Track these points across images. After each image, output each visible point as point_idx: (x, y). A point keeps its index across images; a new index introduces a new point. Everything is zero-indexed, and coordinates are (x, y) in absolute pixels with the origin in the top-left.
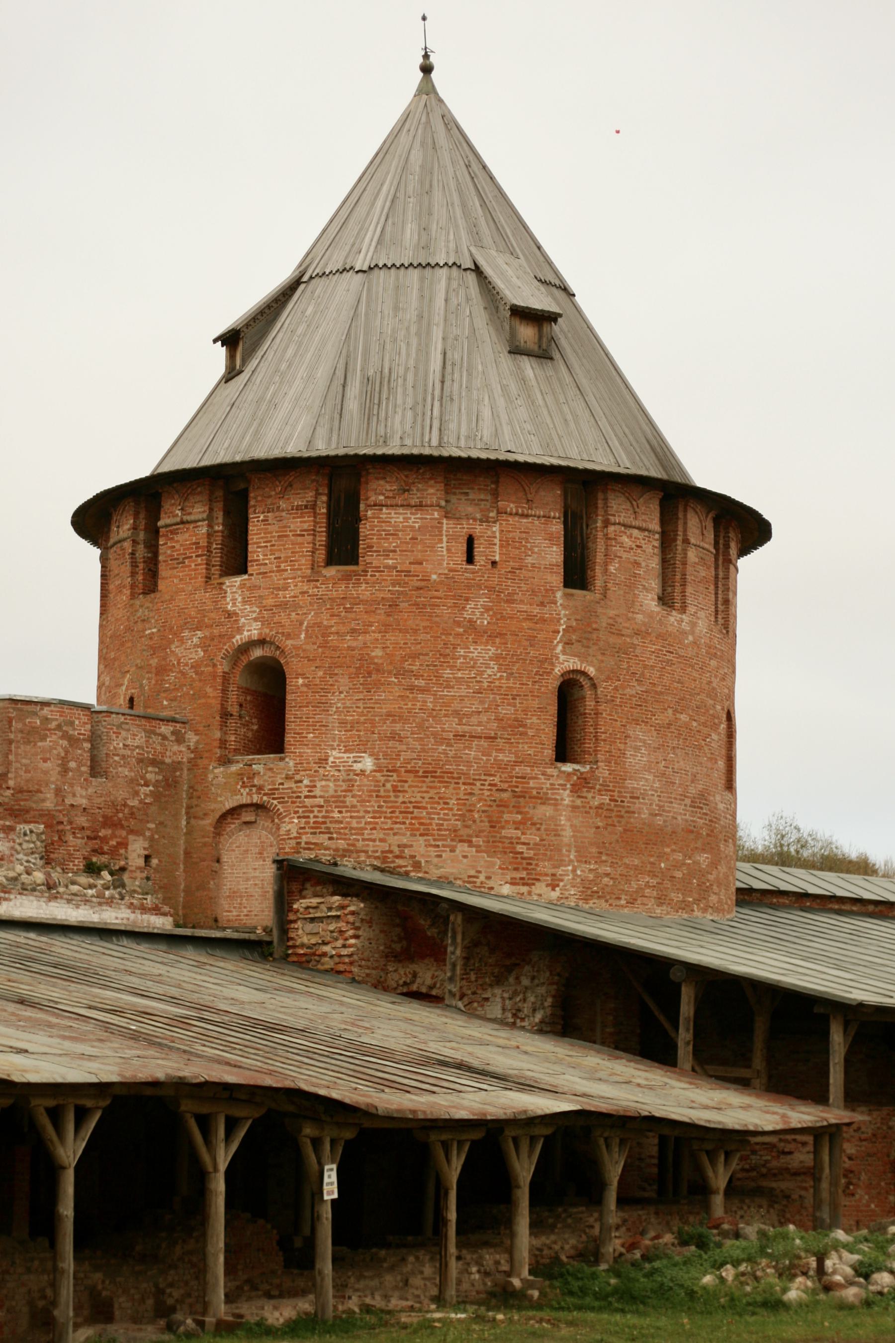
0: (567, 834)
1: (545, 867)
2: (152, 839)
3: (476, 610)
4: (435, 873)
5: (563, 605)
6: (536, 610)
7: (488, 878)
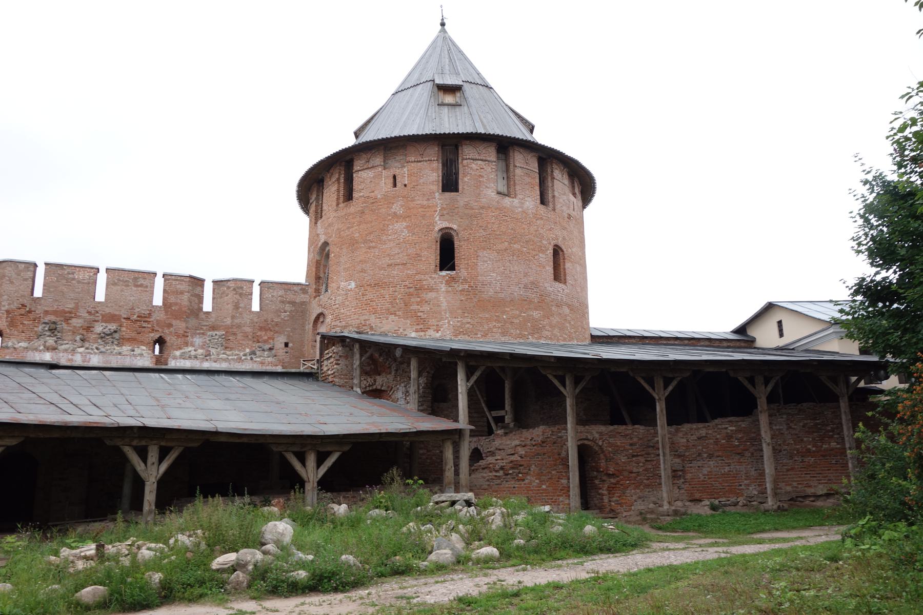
0: (444, 305)
1: (433, 322)
2: (289, 336)
3: (397, 208)
4: (379, 331)
5: (440, 199)
6: (425, 203)
7: (404, 330)
